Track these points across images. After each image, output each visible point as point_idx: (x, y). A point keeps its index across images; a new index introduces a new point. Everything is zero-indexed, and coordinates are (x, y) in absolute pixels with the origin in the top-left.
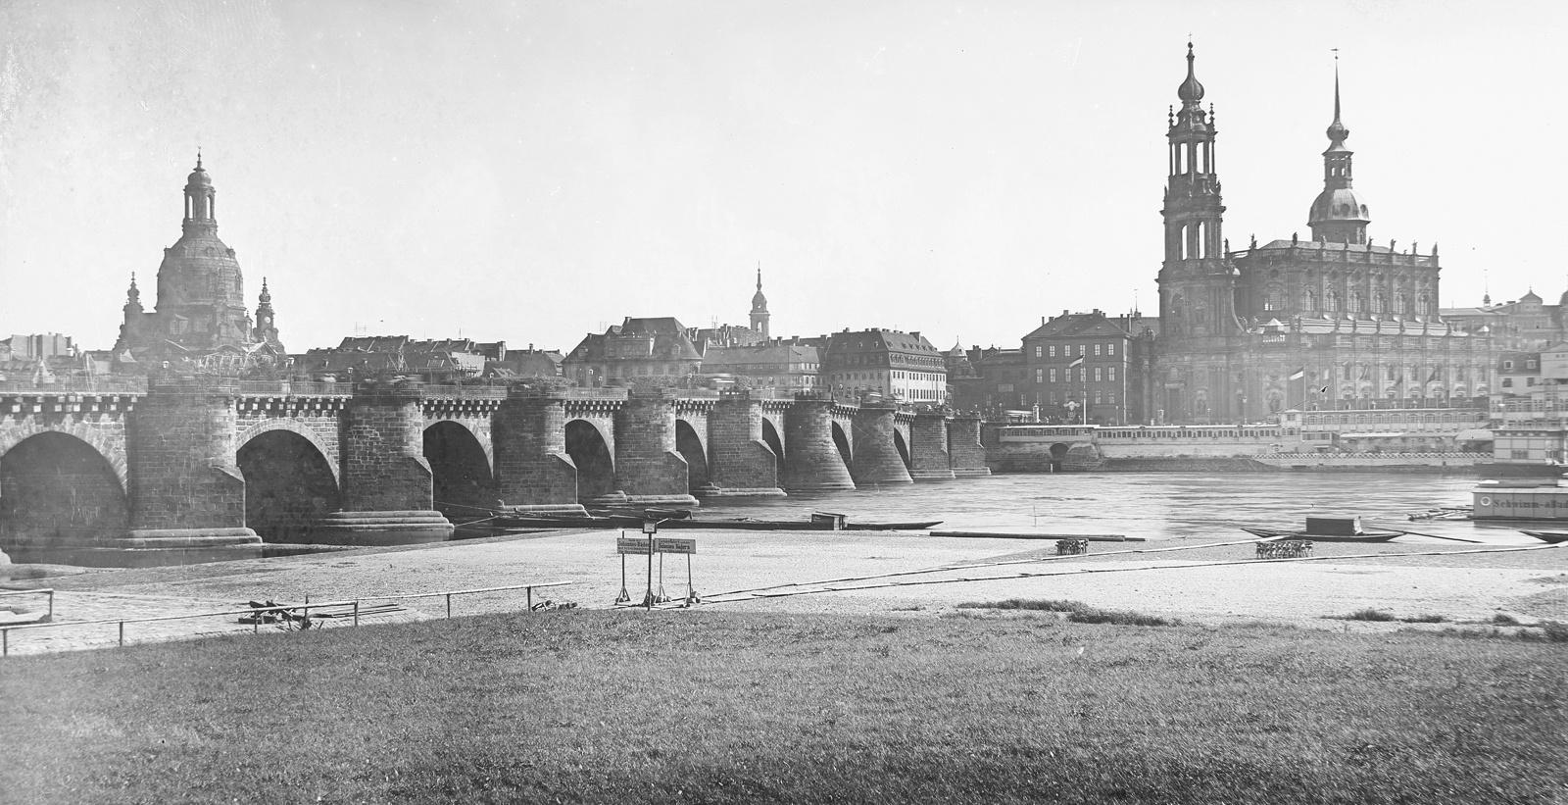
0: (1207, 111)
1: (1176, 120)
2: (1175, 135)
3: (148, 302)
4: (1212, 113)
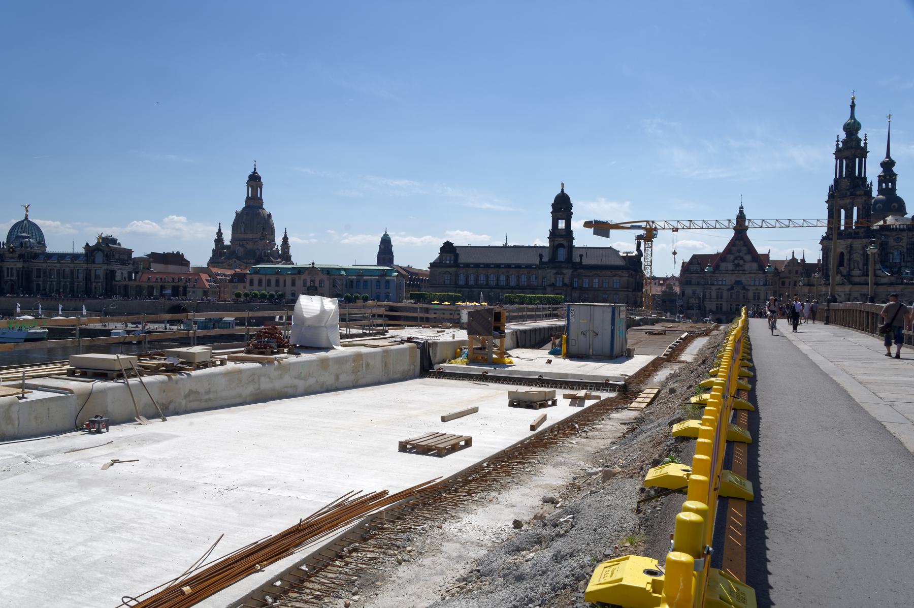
0: (862, 138)
1: (841, 146)
2: (839, 154)
3: (227, 239)
4: (866, 140)
